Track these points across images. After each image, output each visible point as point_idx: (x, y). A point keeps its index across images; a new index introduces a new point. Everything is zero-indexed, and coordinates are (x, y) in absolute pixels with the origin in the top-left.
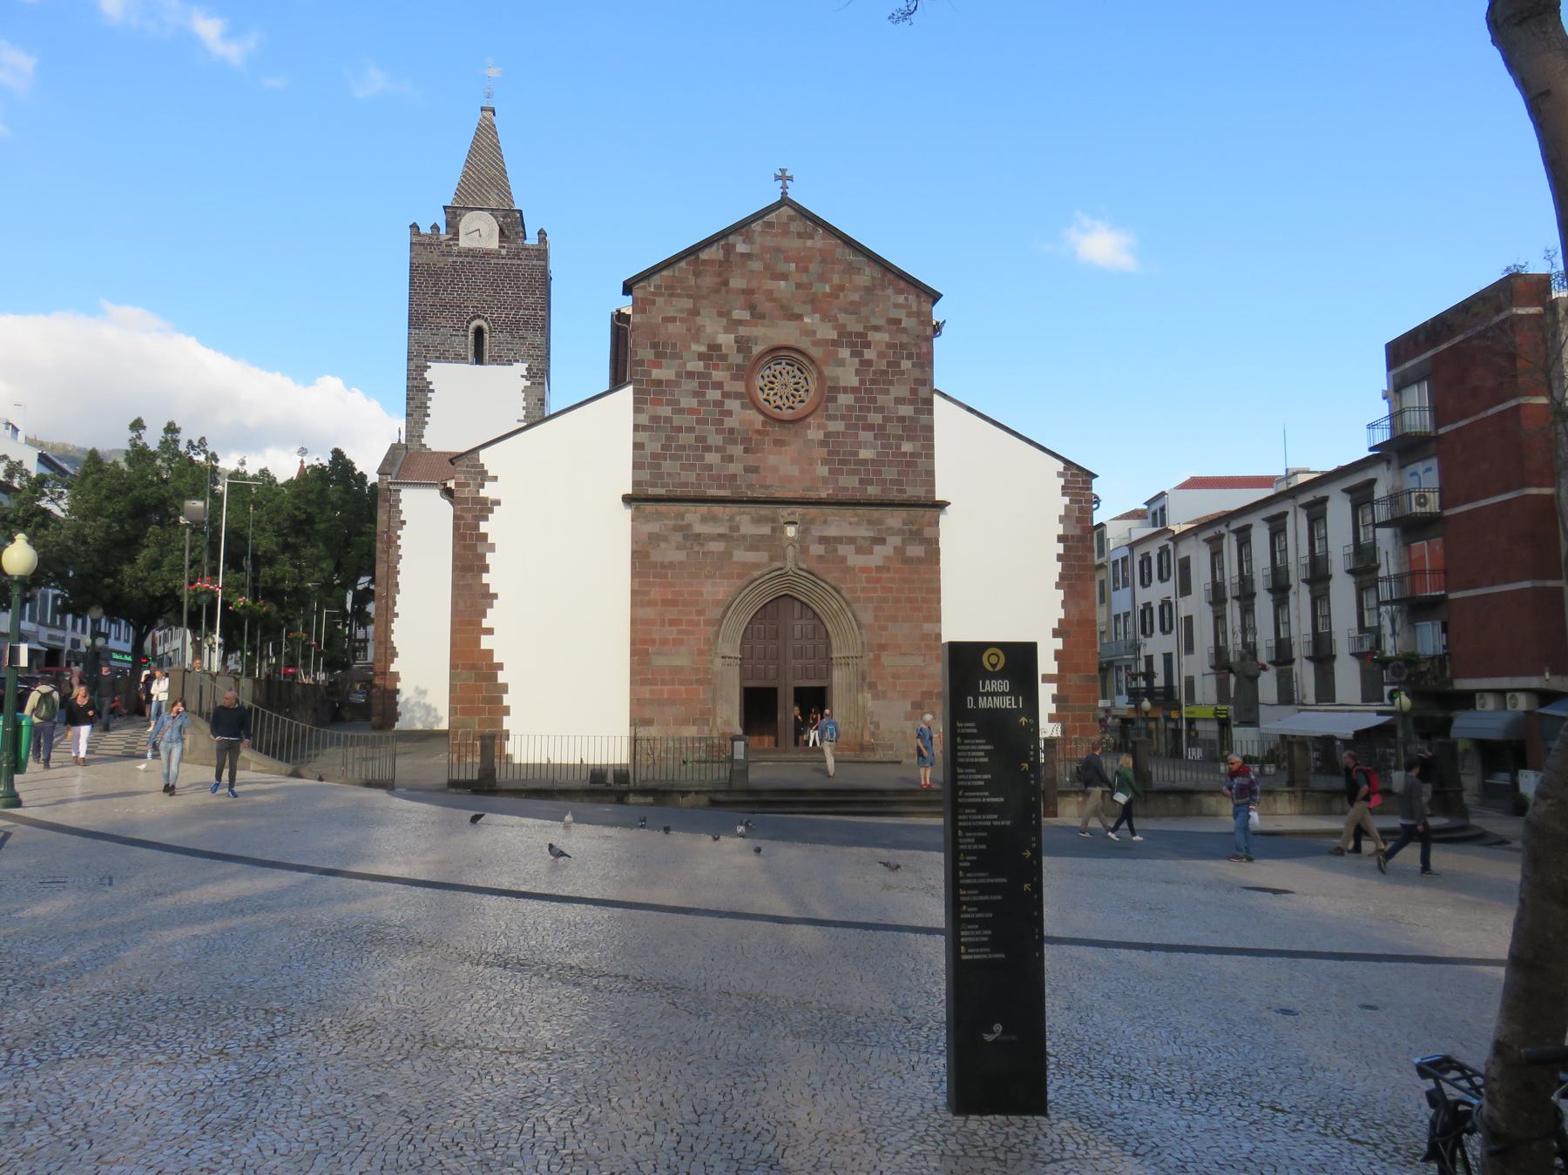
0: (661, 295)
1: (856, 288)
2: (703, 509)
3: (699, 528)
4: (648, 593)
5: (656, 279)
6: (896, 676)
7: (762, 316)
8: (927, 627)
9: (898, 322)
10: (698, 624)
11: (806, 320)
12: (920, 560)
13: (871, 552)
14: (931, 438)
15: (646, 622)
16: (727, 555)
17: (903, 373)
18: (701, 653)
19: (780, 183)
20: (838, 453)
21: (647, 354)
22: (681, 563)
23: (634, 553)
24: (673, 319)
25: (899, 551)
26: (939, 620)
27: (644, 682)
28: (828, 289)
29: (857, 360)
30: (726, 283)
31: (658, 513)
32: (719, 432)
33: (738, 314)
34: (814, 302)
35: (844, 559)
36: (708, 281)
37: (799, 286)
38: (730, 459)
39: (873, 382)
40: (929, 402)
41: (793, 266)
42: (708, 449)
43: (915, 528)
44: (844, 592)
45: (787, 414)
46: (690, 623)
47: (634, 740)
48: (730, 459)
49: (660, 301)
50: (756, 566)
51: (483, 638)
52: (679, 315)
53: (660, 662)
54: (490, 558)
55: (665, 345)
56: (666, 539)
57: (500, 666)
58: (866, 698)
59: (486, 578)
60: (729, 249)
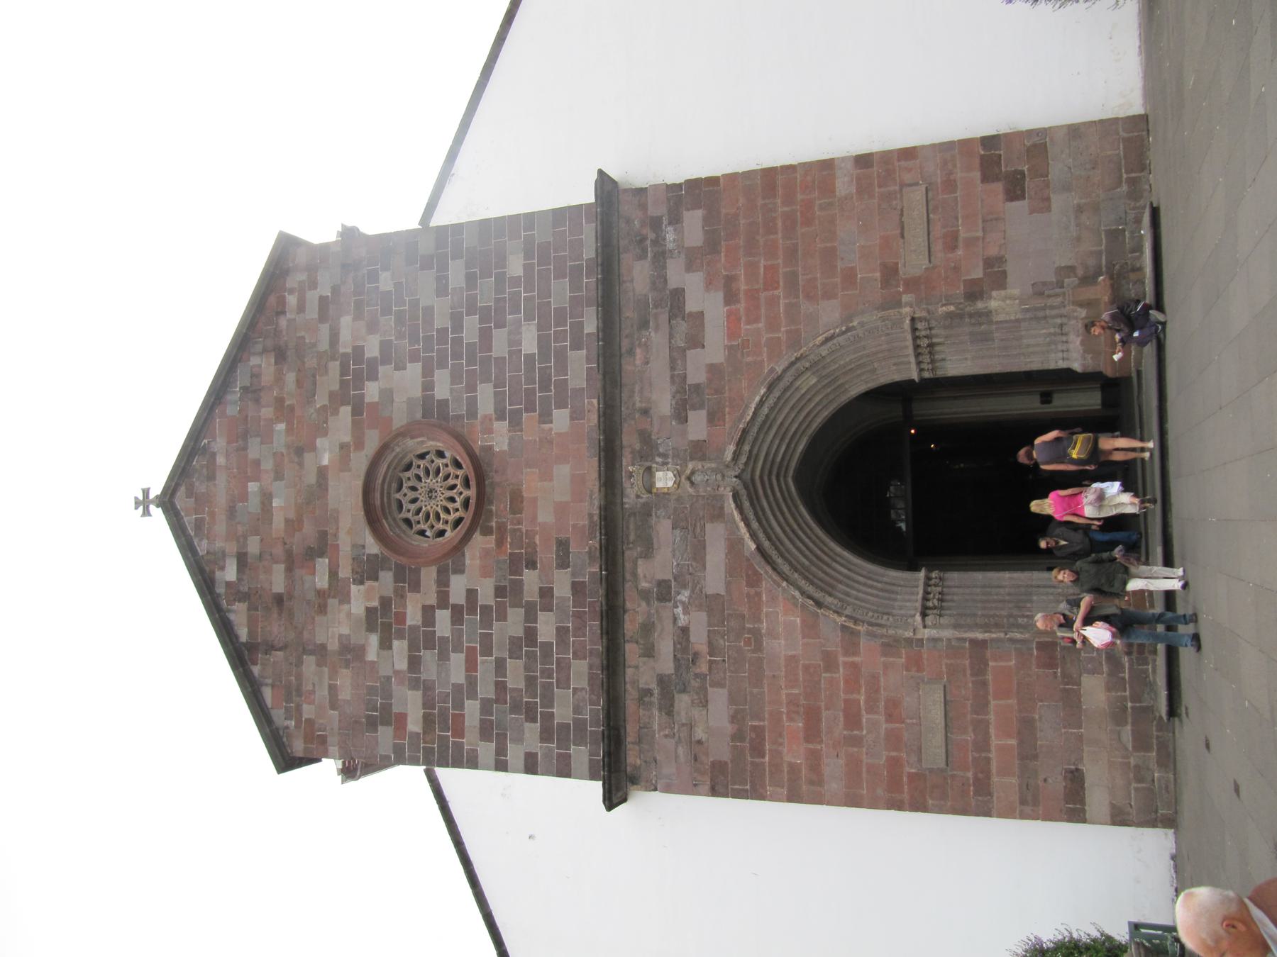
0: (299, 708)
1: (279, 379)
2: (631, 651)
4: (793, 769)
5: (278, 716)
7: (323, 535)
8: (843, 185)
9: (323, 300)
10: (855, 666)
11: (325, 462)
15: (853, 771)
16: (712, 605)
17: (398, 285)
18: (916, 663)
19: (152, 508)
20: (530, 393)
21: (385, 735)
22: (732, 700)
23: (714, 792)
24: (333, 689)
25: (693, 260)
26: (827, 165)
28: (281, 427)
29: (381, 369)
30: (279, 600)
31: (639, 741)
32: (502, 617)
33: (322, 581)
34: (300, 451)
35: (713, 369)
37: (279, 476)
38: (546, 593)
39: (414, 339)
40: (442, 230)
41: (253, 487)
42: (531, 635)
43: (651, 236)
44: (779, 369)
45: (472, 493)
46: (852, 683)
47: (1119, 818)
48: (546, 593)
49: (308, 711)
50: (734, 546)
52: (326, 682)
60: (237, 593)
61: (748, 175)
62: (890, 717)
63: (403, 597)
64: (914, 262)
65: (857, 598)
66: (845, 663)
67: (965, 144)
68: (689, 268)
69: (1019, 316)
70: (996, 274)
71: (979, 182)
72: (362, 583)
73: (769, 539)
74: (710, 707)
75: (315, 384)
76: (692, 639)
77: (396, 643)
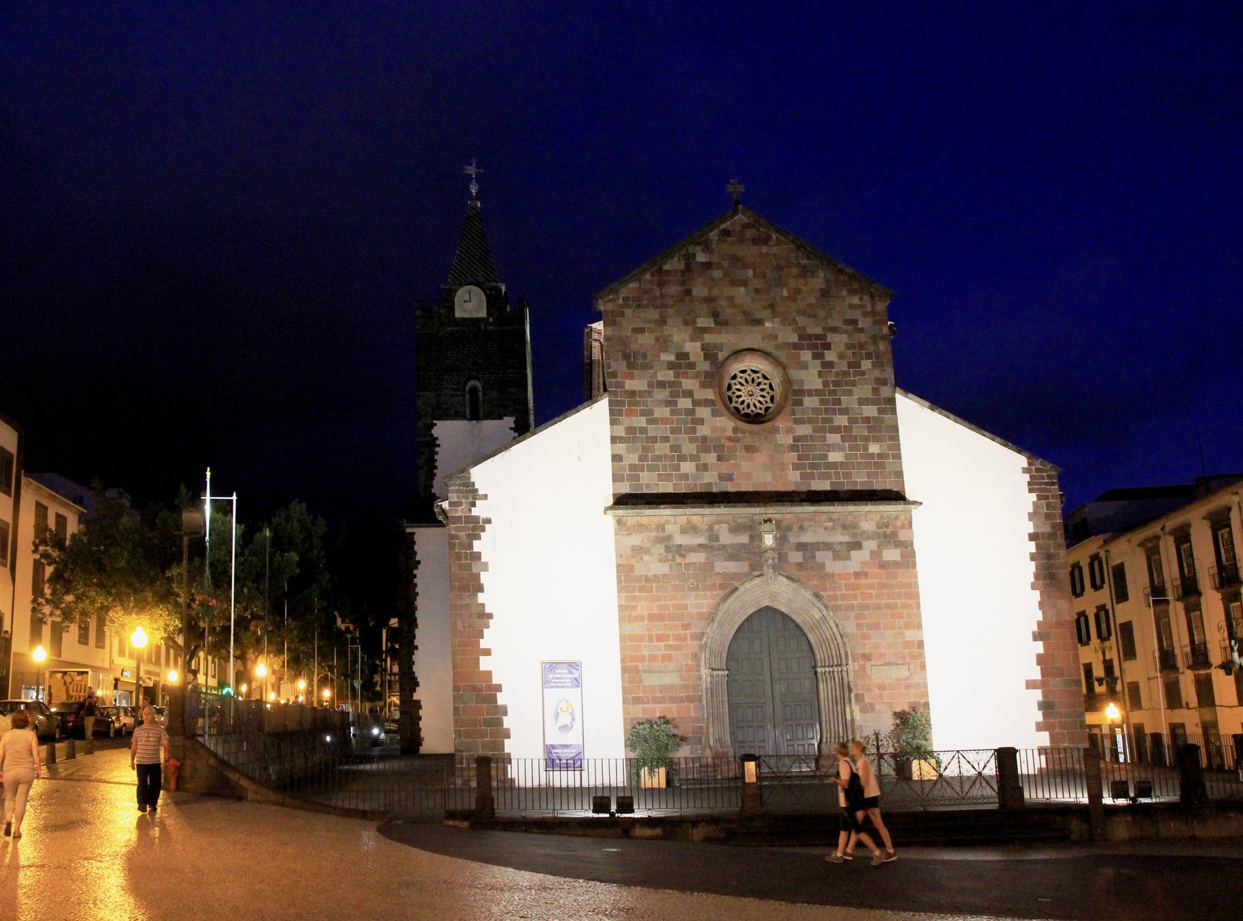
3: (680, 540)
4: (634, 608)
7: (726, 323)
8: (910, 634)
10: (685, 640)
11: (768, 324)
12: (897, 564)
13: (848, 558)
14: (896, 438)
17: (863, 373)
20: (807, 457)
22: (664, 576)
23: (619, 566)
25: (876, 555)
26: (919, 626)
27: (637, 701)
28: (785, 293)
29: (819, 361)
30: (689, 292)
32: (692, 440)
33: (702, 322)
34: (772, 307)
35: (822, 566)
36: (673, 290)
37: (757, 291)
38: (705, 467)
39: (836, 383)
40: (892, 401)
41: (750, 272)
42: (682, 458)
48: (705, 467)
52: (646, 326)
55: (636, 355)
56: (648, 551)
61: (916, 584)
63: (697, 377)
67: (926, 694)
68: (874, 554)
72: (702, 349)
75: (810, 316)
76: (692, 554)
77: (671, 372)
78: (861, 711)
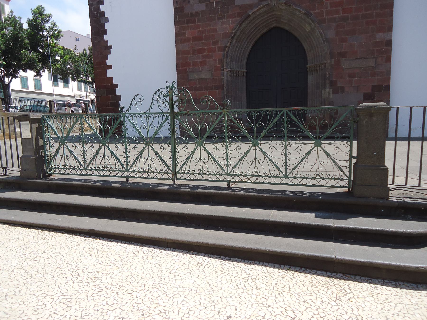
4: (184, 34)
6: (351, 76)
8: (380, 36)
10: (215, 51)
22: (203, 11)
23: (175, 9)
26: (390, 29)
51: (108, 71)
53: (194, 76)
54: (107, 26)
57: (116, 86)
58: (327, 92)
59: (106, 38)
62: (201, 62)
64: (346, 64)
65: (235, 50)
66: (215, 47)
67: (388, 79)
69: (323, 98)
70: (337, 90)
71: (373, 84)
73: (253, 19)
74: (200, 4)
78: (333, 92)
